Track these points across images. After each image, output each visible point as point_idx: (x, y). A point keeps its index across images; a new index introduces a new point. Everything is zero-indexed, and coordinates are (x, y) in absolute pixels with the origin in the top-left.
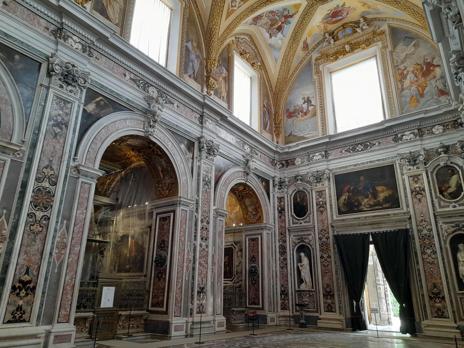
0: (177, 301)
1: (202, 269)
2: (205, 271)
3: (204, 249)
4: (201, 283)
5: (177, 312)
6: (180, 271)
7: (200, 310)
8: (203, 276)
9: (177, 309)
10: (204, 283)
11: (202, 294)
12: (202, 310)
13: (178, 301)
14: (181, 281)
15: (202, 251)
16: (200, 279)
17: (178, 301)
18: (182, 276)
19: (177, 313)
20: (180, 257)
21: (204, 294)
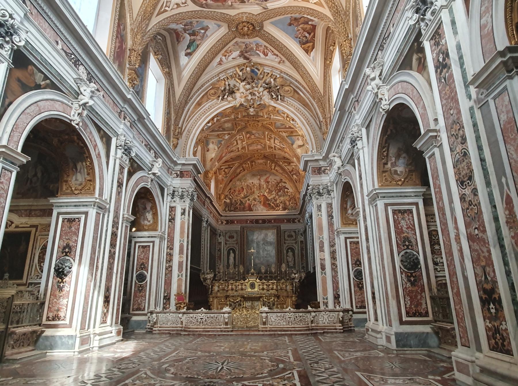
0: (459, 318)
1: (478, 248)
2: (485, 250)
3: (470, 203)
4: (483, 278)
5: (463, 337)
6: (451, 263)
7: (496, 343)
8: (483, 264)
9: (462, 332)
10: (489, 279)
11: (492, 306)
12: (503, 345)
13: (461, 316)
14: (456, 280)
15: (468, 209)
16: (479, 271)
17: (461, 316)
18: (454, 270)
19: (463, 340)
20: (445, 238)
21: (498, 307)
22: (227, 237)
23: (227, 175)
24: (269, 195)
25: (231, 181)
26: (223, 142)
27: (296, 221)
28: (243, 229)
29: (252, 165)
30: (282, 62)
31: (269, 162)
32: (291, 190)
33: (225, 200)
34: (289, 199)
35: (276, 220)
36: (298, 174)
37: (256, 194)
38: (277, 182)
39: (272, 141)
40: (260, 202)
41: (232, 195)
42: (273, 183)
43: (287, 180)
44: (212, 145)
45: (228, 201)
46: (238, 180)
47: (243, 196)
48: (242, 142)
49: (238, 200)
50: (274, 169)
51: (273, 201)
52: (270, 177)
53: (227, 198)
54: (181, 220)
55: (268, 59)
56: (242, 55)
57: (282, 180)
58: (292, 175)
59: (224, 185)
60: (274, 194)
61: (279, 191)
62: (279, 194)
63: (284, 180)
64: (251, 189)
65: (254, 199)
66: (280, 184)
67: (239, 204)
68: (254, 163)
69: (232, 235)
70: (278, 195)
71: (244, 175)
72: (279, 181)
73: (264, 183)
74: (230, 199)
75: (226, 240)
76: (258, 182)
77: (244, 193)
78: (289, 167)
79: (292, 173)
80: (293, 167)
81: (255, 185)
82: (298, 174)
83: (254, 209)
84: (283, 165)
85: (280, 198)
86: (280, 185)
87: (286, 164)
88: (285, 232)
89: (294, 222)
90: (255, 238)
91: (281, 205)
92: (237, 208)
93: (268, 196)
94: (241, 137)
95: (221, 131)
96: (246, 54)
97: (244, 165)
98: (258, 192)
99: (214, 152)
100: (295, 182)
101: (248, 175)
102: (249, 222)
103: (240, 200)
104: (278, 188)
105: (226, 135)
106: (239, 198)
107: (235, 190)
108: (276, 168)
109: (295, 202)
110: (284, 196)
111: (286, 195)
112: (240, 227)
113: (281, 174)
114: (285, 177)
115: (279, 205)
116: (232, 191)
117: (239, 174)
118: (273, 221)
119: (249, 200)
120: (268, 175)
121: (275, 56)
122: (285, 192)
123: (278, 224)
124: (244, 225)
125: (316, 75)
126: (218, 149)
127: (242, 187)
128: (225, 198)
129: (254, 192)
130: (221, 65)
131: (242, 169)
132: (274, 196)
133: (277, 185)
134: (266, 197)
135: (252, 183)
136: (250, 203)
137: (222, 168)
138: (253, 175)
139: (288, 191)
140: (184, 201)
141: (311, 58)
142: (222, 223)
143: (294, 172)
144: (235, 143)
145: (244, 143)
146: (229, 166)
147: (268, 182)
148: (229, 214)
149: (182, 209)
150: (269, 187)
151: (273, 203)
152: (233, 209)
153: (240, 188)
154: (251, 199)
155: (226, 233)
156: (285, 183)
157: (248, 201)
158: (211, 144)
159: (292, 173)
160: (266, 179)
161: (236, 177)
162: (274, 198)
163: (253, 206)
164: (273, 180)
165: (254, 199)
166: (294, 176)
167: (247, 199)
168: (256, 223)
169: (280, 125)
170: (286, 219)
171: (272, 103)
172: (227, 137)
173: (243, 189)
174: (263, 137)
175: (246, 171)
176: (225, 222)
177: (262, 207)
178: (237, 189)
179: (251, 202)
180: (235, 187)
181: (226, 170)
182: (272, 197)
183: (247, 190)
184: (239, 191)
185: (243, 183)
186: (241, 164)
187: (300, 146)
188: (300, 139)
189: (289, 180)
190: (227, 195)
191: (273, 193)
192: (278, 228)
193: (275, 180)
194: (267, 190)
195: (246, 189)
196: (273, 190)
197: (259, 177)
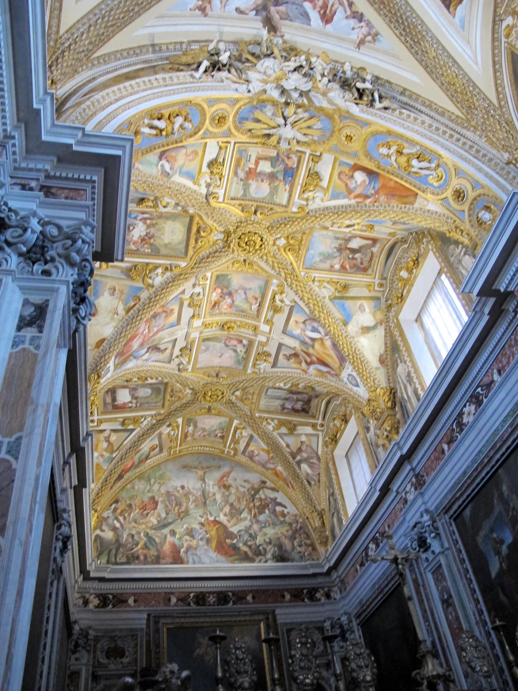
22: (98, 653)
23: (112, 452)
24: (232, 522)
25: (120, 477)
26: (144, 295)
27: (318, 595)
28: (157, 623)
29: (186, 436)
30: (369, 38)
31: (236, 422)
32: (291, 509)
33: (98, 532)
34: (290, 533)
35: (257, 594)
36: (315, 461)
37: (195, 518)
38: (253, 488)
39: (280, 319)
40: (208, 541)
41: (121, 519)
42: (242, 489)
43: (281, 483)
44: (110, 298)
45: (108, 535)
46: (140, 477)
47: (155, 522)
48: (193, 316)
49: (139, 533)
50: (244, 453)
51: (246, 537)
52: (232, 475)
53: (104, 527)
54: (15, 344)
55: (328, 35)
56: (265, 8)
57: (264, 482)
58: (299, 463)
59: (99, 485)
60: (246, 519)
61: (261, 511)
62: (262, 518)
63: (269, 484)
64: (179, 504)
65: (190, 533)
66: (261, 492)
67: (142, 543)
68: (191, 429)
69: (120, 643)
70: (258, 522)
71: (159, 465)
72: (256, 486)
73: (216, 488)
74: (114, 529)
75: (97, 665)
76: (199, 485)
77: (159, 516)
78: (290, 440)
79: (298, 458)
80: (304, 438)
81: (189, 493)
82: (315, 461)
83: (191, 560)
84: (275, 433)
85: (264, 530)
86: (261, 494)
87: (284, 430)
88: (289, 631)
89: (312, 597)
90: (199, 651)
91: (271, 550)
92: (138, 558)
93: (228, 525)
94: (198, 289)
95: (148, 255)
96: (273, 9)
97: (165, 430)
98: (201, 512)
99: (112, 319)
100: (306, 483)
101: (170, 466)
102: (174, 600)
103: (147, 535)
104: (258, 504)
105: (159, 271)
106: (144, 526)
107: (130, 506)
108: (251, 448)
109: (308, 542)
110: (274, 525)
111: (282, 522)
112: (145, 616)
113: (264, 466)
114: (276, 474)
115: (265, 550)
116: (121, 506)
117: (147, 458)
118: (249, 598)
119: (173, 533)
120: (226, 469)
121: (353, 22)
122: (276, 515)
123: (269, 606)
124: (161, 608)
125: (470, 62)
126: (128, 311)
127: (153, 498)
128: (99, 526)
129: (187, 513)
130: (206, 15)
131: (156, 442)
132: (247, 523)
133: (253, 496)
134: (225, 527)
135: (183, 487)
136: (177, 542)
137: (102, 427)
138: (184, 467)
139: (286, 511)
140: (46, 273)
141: (457, 20)
142: (86, 603)
143: (305, 455)
144: (174, 318)
145: (197, 323)
146: (123, 423)
147: (227, 487)
148: (113, 571)
149: (26, 302)
150: (232, 499)
151: (245, 544)
152: (124, 560)
153: (146, 500)
154: (180, 530)
155: (97, 639)
156: (273, 489)
157: (169, 538)
158: (106, 293)
159: (298, 458)
160: (222, 478)
161: (137, 466)
162: (247, 529)
163: (186, 552)
164: (240, 482)
165: (190, 533)
166: (304, 467)
167: (166, 531)
168: (197, 603)
169: (317, 259)
170: (287, 590)
171: (356, 110)
172: (158, 280)
173: (156, 503)
174: (255, 307)
175: (165, 454)
176: (96, 602)
177: (213, 555)
178: (137, 502)
179: (180, 539)
180: (132, 498)
181: (113, 438)
182: (242, 526)
183: (166, 506)
184: (144, 508)
185: (156, 487)
186: (160, 423)
187: (366, 330)
188: (367, 310)
189: (285, 480)
190: (106, 519)
191: (245, 514)
192: (267, 618)
193: (245, 481)
194: (227, 509)
195: (163, 502)
196: (243, 507)
197: (200, 473)
